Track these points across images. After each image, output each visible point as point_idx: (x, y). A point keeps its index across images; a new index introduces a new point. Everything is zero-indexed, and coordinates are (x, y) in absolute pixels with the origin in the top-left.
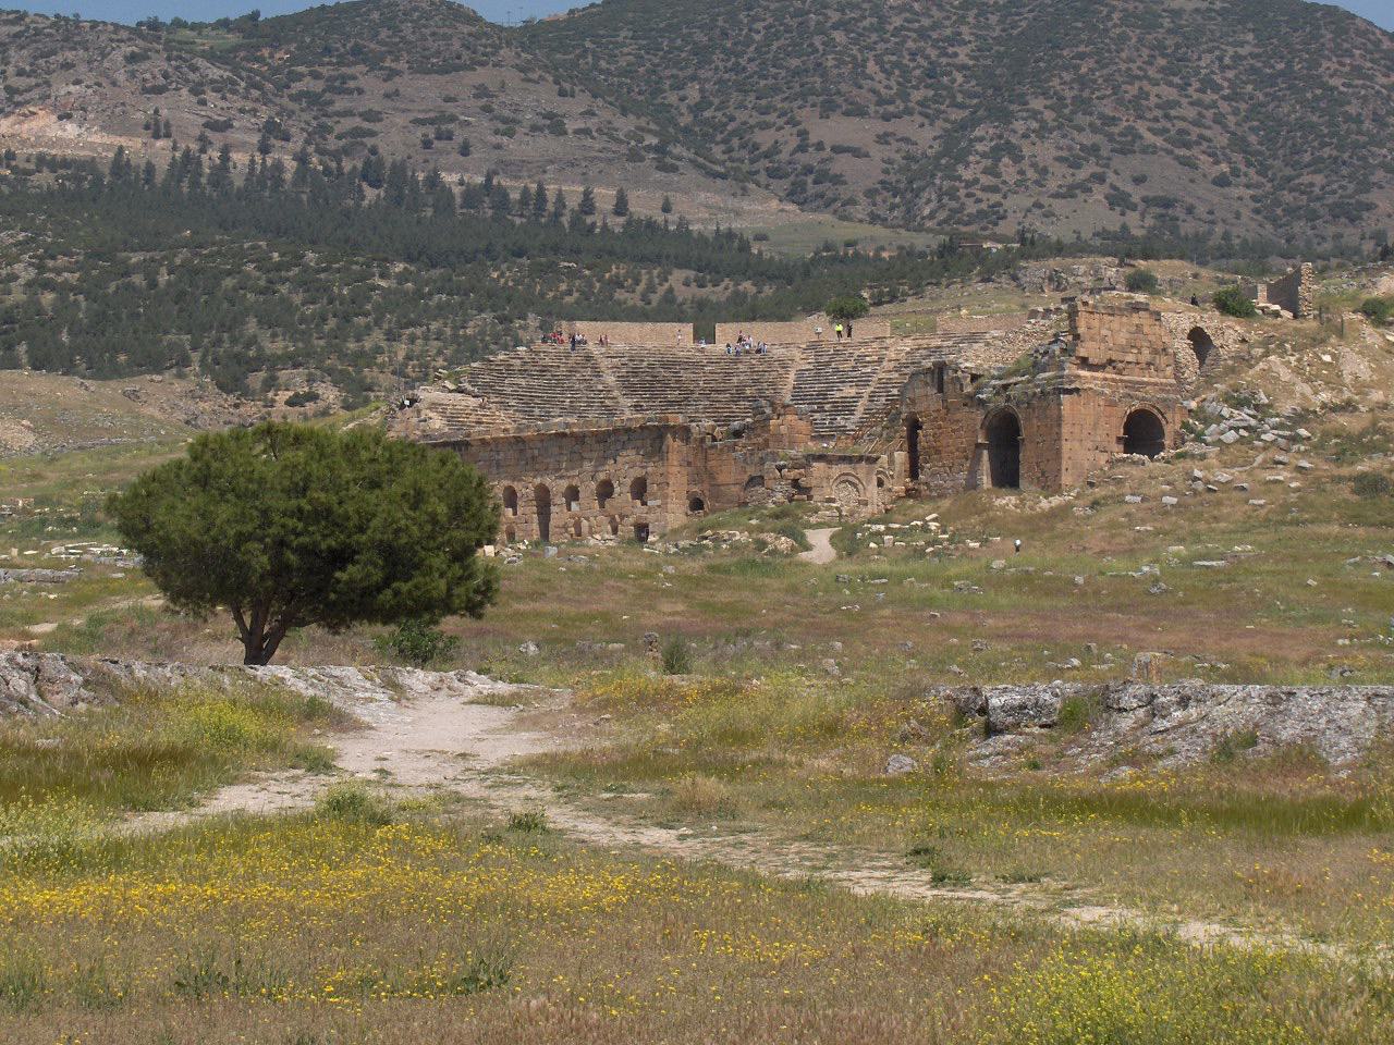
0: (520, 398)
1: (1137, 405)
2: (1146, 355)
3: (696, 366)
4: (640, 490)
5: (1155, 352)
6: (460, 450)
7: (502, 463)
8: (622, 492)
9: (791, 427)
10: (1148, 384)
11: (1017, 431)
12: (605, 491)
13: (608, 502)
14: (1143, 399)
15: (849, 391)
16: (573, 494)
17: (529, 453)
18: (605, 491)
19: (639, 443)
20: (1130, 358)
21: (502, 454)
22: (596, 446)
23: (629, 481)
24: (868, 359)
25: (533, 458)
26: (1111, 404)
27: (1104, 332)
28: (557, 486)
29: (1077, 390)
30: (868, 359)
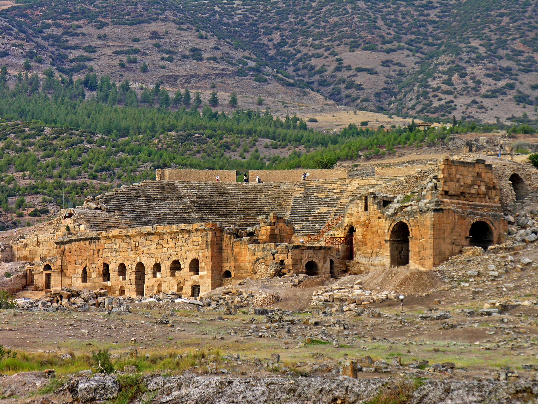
0: (133, 212)
1: (477, 219)
2: (483, 188)
3: (236, 195)
4: (195, 266)
5: (488, 188)
6: (95, 242)
7: (118, 250)
8: (185, 265)
9: (281, 230)
10: (484, 206)
11: (408, 233)
12: (176, 266)
13: (177, 273)
14: (481, 215)
15: (324, 210)
16: (157, 267)
17: (133, 244)
18: (176, 266)
19: (195, 239)
20: (473, 191)
21: (118, 245)
22: (170, 241)
23: (189, 260)
24: (335, 191)
26: (462, 218)
27: (458, 176)
28: (149, 264)
29: (442, 210)
30: (335, 191)
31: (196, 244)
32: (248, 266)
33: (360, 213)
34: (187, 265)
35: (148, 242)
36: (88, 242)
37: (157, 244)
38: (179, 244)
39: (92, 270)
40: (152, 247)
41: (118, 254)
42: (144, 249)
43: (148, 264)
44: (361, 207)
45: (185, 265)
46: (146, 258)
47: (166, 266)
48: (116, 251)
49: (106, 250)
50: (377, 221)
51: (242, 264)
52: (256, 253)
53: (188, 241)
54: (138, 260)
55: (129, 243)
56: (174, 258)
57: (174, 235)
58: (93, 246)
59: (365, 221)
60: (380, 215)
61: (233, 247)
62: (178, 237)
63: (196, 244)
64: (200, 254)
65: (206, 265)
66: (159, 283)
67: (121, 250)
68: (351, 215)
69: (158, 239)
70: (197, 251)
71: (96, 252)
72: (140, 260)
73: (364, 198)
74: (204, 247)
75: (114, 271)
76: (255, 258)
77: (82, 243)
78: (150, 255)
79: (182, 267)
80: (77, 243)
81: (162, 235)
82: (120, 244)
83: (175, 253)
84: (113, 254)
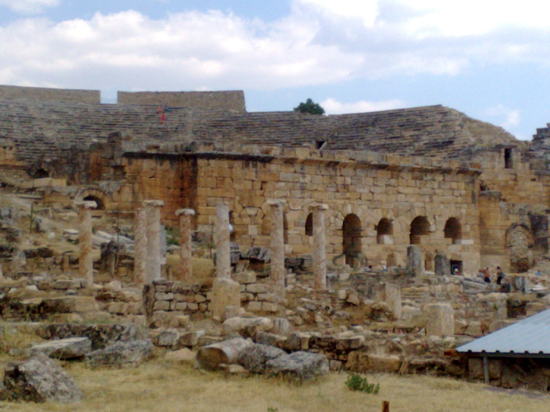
6: (255, 166)
7: (308, 186)
8: (437, 228)
16: (384, 227)
17: (340, 180)
19: (454, 185)
21: (308, 179)
22: (412, 182)
25: (345, 186)
28: (369, 218)
31: (456, 193)
32: (500, 234)
33: (496, 170)
34: (442, 227)
35: (370, 181)
36: (238, 164)
37: (387, 185)
38: (427, 189)
39: (247, 220)
40: (377, 190)
41: (307, 194)
42: (362, 190)
43: (368, 219)
44: (500, 162)
45: (437, 228)
46: (365, 207)
47: (401, 226)
48: (303, 189)
49: (282, 184)
50: (530, 185)
51: (491, 232)
52: (511, 217)
53: (443, 187)
54: (349, 210)
55: (331, 177)
56: (418, 213)
57: (420, 173)
58: (251, 172)
59: (507, 182)
60: (534, 177)
62: (425, 178)
63: (456, 193)
64: (464, 211)
65: (472, 229)
66: (390, 253)
67: (315, 187)
69: (389, 176)
70: (459, 205)
71: (258, 185)
72: (352, 209)
73: (503, 150)
74: (470, 199)
75: (296, 224)
76: (509, 223)
77: (225, 164)
78: (373, 204)
79: (433, 228)
80: (212, 162)
81: (395, 170)
82: (314, 178)
83: (422, 205)
84: (298, 193)
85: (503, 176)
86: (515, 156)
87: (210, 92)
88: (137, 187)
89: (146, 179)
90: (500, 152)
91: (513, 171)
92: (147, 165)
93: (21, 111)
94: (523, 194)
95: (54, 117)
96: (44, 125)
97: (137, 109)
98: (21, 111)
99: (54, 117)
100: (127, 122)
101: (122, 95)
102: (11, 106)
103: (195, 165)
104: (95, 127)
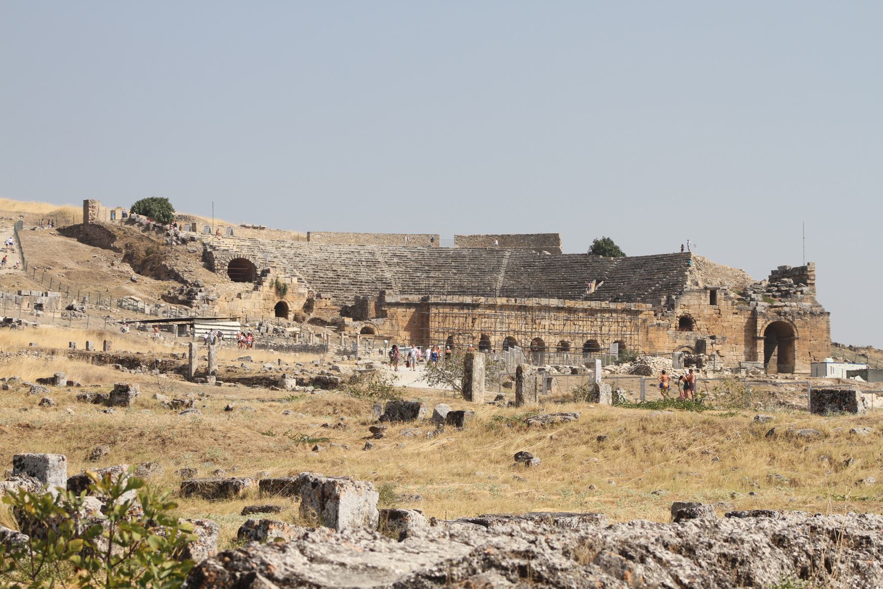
16: (564, 347)
50: (731, 317)
52: (678, 341)
57: (592, 312)
60: (735, 311)
61: (647, 332)
68: (688, 307)
76: (676, 345)
85: (708, 310)
86: (719, 296)
87: (532, 235)
88: (394, 321)
89: (400, 317)
90: (706, 293)
91: (717, 307)
92: (400, 310)
93: (370, 257)
94: (725, 324)
95: (396, 260)
96: (385, 267)
97: (465, 252)
98: (370, 257)
99: (396, 260)
100: (453, 264)
101: (459, 238)
102: (362, 252)
103: (428, 310)
104: (427, 268)
